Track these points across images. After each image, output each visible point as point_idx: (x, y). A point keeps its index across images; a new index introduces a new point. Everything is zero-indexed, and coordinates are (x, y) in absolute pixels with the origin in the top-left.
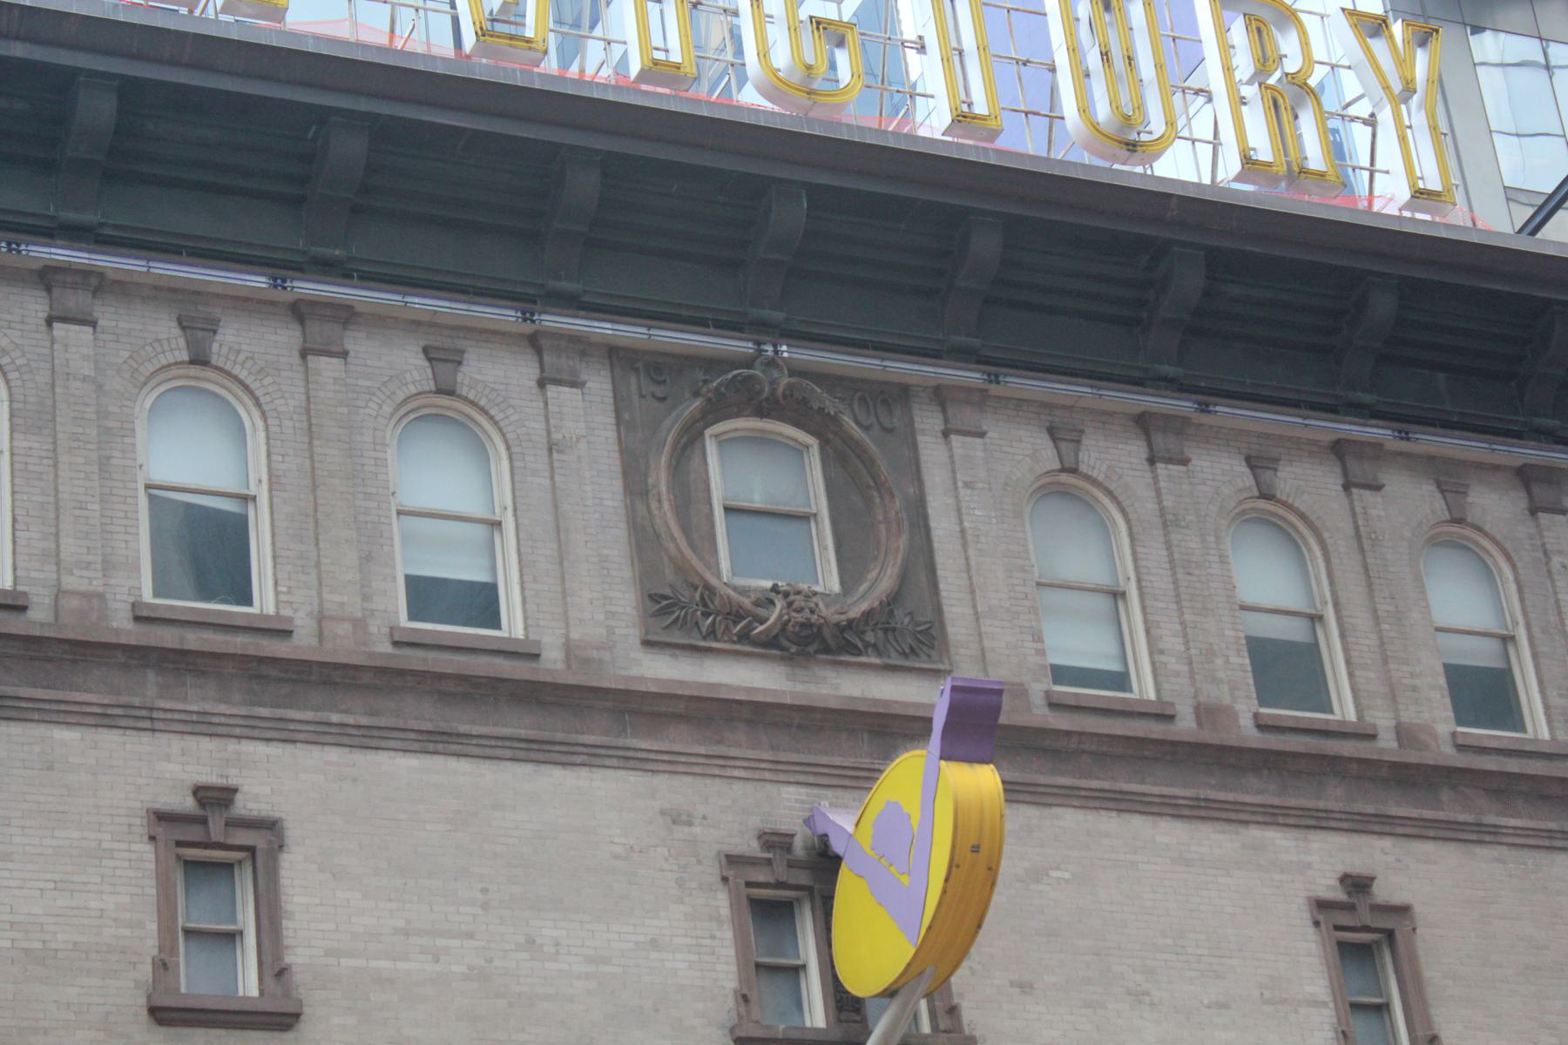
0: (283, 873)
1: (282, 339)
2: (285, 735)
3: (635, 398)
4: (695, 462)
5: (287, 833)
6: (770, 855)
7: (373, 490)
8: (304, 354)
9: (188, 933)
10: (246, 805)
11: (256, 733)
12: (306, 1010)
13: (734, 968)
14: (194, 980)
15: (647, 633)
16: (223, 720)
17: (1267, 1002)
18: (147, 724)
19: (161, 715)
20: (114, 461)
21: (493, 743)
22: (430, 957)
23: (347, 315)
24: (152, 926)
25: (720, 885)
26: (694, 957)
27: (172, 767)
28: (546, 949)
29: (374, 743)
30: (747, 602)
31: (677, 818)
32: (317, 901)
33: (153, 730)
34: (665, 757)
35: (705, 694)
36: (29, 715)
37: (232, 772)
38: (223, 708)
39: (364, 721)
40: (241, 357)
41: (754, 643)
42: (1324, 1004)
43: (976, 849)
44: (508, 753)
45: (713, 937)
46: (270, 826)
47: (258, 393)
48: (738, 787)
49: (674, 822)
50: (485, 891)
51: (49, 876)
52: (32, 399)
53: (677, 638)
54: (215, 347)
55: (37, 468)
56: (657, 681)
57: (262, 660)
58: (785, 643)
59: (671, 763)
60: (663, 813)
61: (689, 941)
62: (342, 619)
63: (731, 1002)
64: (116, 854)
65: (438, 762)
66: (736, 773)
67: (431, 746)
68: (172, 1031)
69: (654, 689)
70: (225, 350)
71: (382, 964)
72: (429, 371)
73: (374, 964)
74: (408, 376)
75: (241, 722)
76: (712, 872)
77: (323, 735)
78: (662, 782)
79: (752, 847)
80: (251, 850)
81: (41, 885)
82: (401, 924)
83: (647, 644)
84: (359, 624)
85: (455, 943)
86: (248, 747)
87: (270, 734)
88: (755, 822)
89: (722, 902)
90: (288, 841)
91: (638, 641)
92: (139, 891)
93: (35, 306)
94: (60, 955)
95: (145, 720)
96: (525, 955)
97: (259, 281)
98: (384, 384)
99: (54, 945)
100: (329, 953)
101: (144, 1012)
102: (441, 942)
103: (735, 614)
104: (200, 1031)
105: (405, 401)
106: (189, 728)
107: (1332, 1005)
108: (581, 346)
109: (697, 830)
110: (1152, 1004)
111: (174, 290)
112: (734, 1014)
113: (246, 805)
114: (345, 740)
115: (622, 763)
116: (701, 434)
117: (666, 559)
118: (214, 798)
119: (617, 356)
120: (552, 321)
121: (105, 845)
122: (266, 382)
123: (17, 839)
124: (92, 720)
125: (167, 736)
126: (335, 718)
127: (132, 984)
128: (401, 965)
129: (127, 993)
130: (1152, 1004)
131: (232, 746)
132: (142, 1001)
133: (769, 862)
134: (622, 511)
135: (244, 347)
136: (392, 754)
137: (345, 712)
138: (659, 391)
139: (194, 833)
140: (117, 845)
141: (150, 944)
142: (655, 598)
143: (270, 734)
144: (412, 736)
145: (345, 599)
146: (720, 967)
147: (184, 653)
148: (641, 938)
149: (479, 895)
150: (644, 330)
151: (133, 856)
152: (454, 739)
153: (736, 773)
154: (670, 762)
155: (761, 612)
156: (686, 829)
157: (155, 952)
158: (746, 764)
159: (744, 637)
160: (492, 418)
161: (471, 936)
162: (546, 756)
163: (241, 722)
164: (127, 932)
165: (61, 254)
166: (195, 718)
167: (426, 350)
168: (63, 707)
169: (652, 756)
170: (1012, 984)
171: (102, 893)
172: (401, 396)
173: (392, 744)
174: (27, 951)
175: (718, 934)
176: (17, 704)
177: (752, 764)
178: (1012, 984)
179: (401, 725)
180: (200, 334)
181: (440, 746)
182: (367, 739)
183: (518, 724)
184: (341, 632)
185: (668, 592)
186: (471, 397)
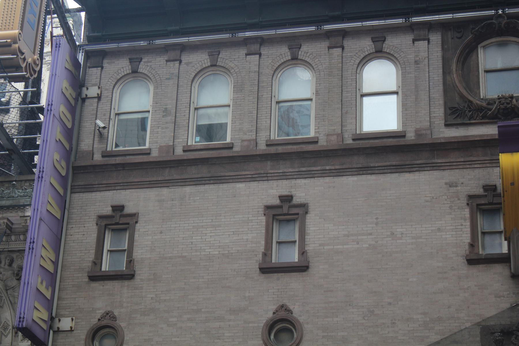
0: (307, 221)
1: (322, 46)
2: (311, 176)
3: (450, 40)
4: (474, 57)
5: (309, 207)
6: (486, 194)
7: (350, 90)
8: (329, 48)
9: (279, 243)
10: (296, 200)
11: (301, 176)
13: (469, 235)
15: (446, 121)
16: (290, 174)
18: (266, 178)
19: (270, 175)
20: (264, 96)
21: (383, 168)
22: (355, 243)
23: (344, 34)
24: (263, 243)
25: (466, 207)
26: (454, 233)
27: (270, 191)
28: (398, 236)
29: (342, 174)
30: (484, 104)
31: (451, 185)
32: (318, 228)
33: (268, 180)
34: (448, 164)
35: (463, 140)
36: (229, 181)
37: (293, 190)
38: (291, 170)
39: (337, 167)
40: (308, 54)
41: (489, 118)
43: (512, 184)
44: (389, 171)
45: (462, 225)
46: (304, 207)
47: (313, 65)
48: (477, 171)
49: (450, 186)
50: (377, 218)
51: (231, 230)
52: (239, 81)
53: (459, 121)
54: (300, 52)
55: (240, 103)
56: (445, 138)
57: (304, 152)
58: (500, 116)
59: (451, 166)
60: (446, 184)
61: (452, 227)
62: (334, 135)
63: (467, 247)
64: (253, 221)
65: (364, 177)
66: (476, 166)
67: (361, 172)
68: (267, 275)
69: (443, 141)
70: (303, 53)
71: (339, 247)
72: (373, 46)
73: (335, 247)
74: (366, 49)
75: (297, 173)
76: (464, 201)
77: (324, 174)
78: (446, 173)
79: (481, 191)
80: (298, 214)
81: (229, 233)
82: (347, 233)
83: (447, 125)
84: (341, 136)
85: (366, 237)
86: (299, 181)
87: (306, 176)
88: (482, 182)
89: (467, 212)
90: (309, 210)
91: (443, 125)
92: (259, 232)
93: (242, 52)
94: (233, 254)
95: (265, 177)
96: (390, 239)
97: (312, 28)
98: (357, 53)
99: (232, 252)
100: (320, 245)
101: (258, 269)
102: (359, 237)
103: (480, 109)
104: (276, 274)
105: (363, 58)
106: (279, 178)
108: (430, 26)
109: (459, 188)
111: (286, 37)
112: (468, 252)
113: (296, 200)
114: (332, 174)
115: (431, 168)
116: (477, 47)
117: (457, 95)
118: (286, 199)
119: (443, 26)
120: (415, 19)
121: (250, 219)
122: (316, 61)
123: (223, 220)
124: (248, 180)
125: (272, 181)
126: (328, 168)
127: (255, 261)
128: (345, 247)
129: (254, 265)
131: (293, 181)
132: (258, 267)
133: (486, 196)
134: (441, 80)
135: (309, 51)
136: (348, 177)
137: (333, 165)
138: (459, 35)
139: (279, 211)
140: (253, 218)
141: (262, 249)
142: (450, 109)
143: (306, 176)
144: (355, 170)
145: (336, 128)
146: (463, 235)
147: (279, 154)
148: (434, 228)
149: (375, 220)
150: (452, 15)
151: (259, 221)
152: (370, 169)
153: (476, 166)
154: (450, 166)
155: (490, 107)
156: (455, 188)
157: (263, 251)
158: (479, 162)
159: (483, 117)
160: (395, 57)
161: (371, 234)
162: (403, 170)
163: (297, 173)
164: (254, 245)
165: (248, 34)
166: (281, 174)
167: (372, 38)
168: (239, 177)
169: (443, 164)
171: (248, 234)
172: (362, 56)
173: (348, 173)
174: (223, 254)
175: (464, 224)
176: (225, 178)
177: (482, 162)
179: (350, 167)
180: (294, 50)
181: (364, 172)
182: (340, 173)
183: (394, 160)
184: (333, 139)
185: (456, 106)
186: (388, 51)
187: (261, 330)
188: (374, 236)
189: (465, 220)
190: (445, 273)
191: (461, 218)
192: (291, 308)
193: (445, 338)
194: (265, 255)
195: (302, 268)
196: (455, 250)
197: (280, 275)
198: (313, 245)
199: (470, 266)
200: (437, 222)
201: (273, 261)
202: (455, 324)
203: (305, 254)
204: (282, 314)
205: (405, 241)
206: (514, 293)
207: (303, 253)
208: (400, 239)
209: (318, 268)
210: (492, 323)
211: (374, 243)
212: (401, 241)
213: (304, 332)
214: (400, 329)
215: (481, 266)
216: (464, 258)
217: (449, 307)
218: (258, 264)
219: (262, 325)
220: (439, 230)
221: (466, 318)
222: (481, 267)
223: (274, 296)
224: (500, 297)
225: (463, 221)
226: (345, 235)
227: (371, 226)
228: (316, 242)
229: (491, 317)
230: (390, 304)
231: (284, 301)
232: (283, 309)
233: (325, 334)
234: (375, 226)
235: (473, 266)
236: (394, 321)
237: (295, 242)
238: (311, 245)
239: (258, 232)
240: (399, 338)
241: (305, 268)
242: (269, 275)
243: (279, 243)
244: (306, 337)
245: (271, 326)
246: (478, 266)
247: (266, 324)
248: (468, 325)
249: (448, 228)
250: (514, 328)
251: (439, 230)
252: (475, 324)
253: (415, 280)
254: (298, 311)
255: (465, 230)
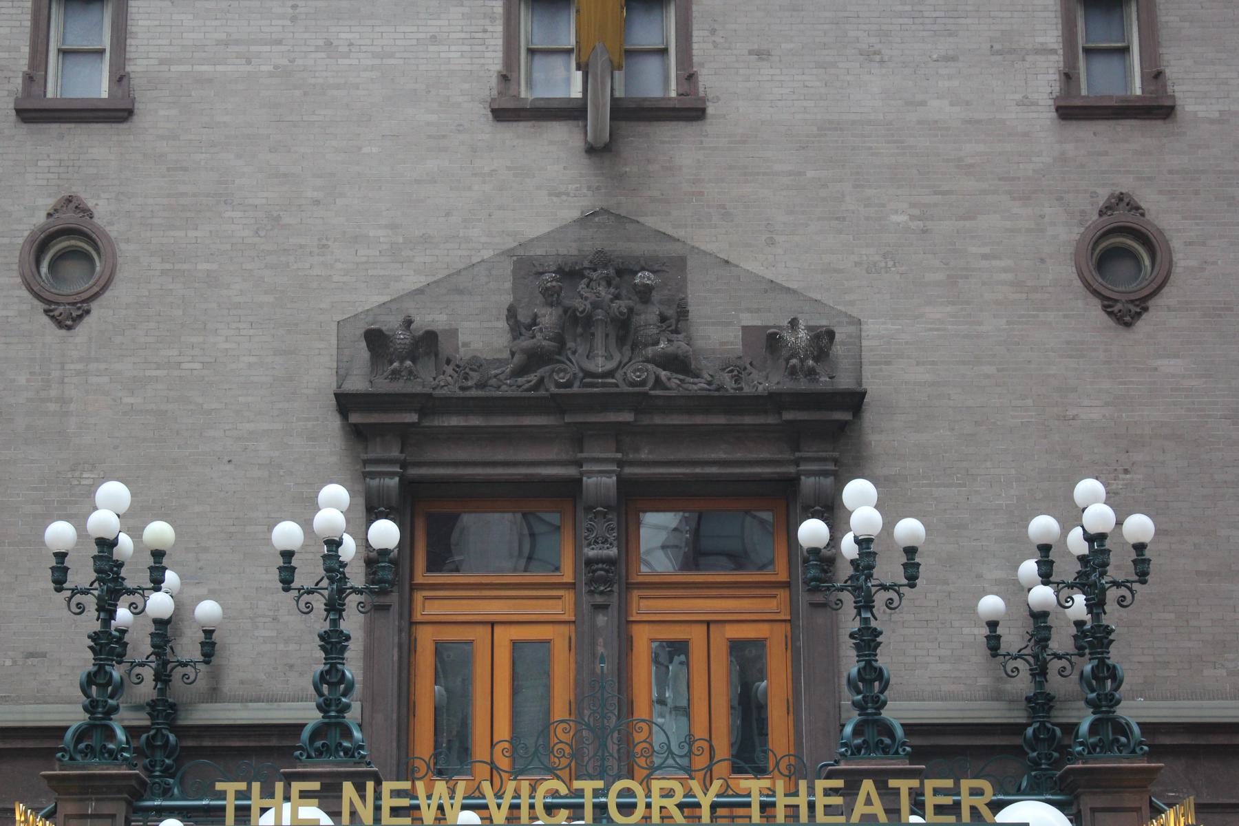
9: (64, 53)
12: (138, 106)
13: (500, 55)
14: (1100, 81)
17: (999, 53)
22: (244, 61)
24: (26, 50)
26: (467, 48)
28: (340, 49)
32: (157, 23)
42: (1054, 51)
45: (485, 31)
50: (294, 7)
61: (463, 35)
73: (197, 68)
82: (224, 36)
85: (268, 48)
92: (18, 24)
96: (323, 55)
100: (162, 62)
102: (253, 48)
107: (1061, 52)
110: (882, 61)
112: (495, 93)
127: (6, 93)
128: (219, 68)
130: (882, 61)
132: (12, 106)
141: (23, 64)
146: (487, 55)
149: (290, 11)
157: (26, 69)
161: (279, 42)
170: (751, 52)
175: (490, 28)
178: (751, 52)
187: (17, 253)
188: (287, 48)
189: (493, 19)
190: (444, 137)
191: (485, 16)
192: (90, 204)
193: (435, 282)
194: (29, 79)
195: (116, 114)
196: (466, 86)
197: (65, 127)
198: (145, 62)
199: (499, 124)
200: (430, 22)
201: (50, 95)
202: (460, 253)
203: (125, 81)
204: (68, 218)
205: (355, 62)
206: (589, 188)
207: (120, 78)
208: (346, 56)
209: (155, 113)
210: (540, 252)
211: (285, 62)
212: (347, 61)
213: (120, 260)
214: (337, 260)
215: (521, 124)
216: (487, 105)
217: (447, 215)
218: (12, 100)
219: (21, 241)
220: (434, 39)
221: (483, 239)
222: (522, 127)
223: (51, 176)
224: (558, 195)
225: (488, 21)
226: (219, 43)
227: (280, 22)
228: (151, 55)
229: (538, 239)
230: (317, 202)
231: (74, 189)
232: (72, 205)
233: (168, 266)
234: (289, 23)
235: (505, 124)
236: (324, 242)
237: (101, 52)
238: (138, 61)
239: (14, 23)
240: (335, 279)
241: (126, 114)
242: (40, 126)
243: (64, 53)
244: (125, 272)
245: (42, 244)
246: (515, 124)
247: (31, 240)
248: (487, 254)
249: (452, 36)
250: (586, 264)
251: (434, 39)
252: (503, 253)
253: (374, 150)
254: (105, 212)
255: (492, 42)
